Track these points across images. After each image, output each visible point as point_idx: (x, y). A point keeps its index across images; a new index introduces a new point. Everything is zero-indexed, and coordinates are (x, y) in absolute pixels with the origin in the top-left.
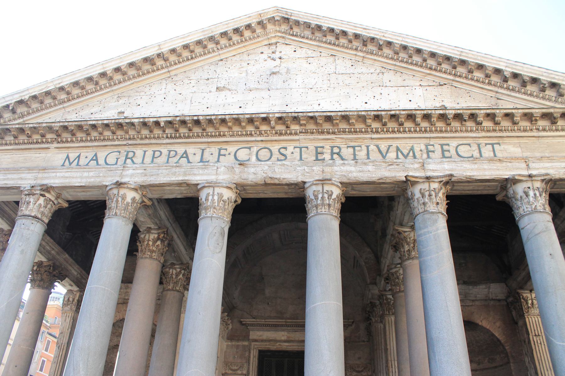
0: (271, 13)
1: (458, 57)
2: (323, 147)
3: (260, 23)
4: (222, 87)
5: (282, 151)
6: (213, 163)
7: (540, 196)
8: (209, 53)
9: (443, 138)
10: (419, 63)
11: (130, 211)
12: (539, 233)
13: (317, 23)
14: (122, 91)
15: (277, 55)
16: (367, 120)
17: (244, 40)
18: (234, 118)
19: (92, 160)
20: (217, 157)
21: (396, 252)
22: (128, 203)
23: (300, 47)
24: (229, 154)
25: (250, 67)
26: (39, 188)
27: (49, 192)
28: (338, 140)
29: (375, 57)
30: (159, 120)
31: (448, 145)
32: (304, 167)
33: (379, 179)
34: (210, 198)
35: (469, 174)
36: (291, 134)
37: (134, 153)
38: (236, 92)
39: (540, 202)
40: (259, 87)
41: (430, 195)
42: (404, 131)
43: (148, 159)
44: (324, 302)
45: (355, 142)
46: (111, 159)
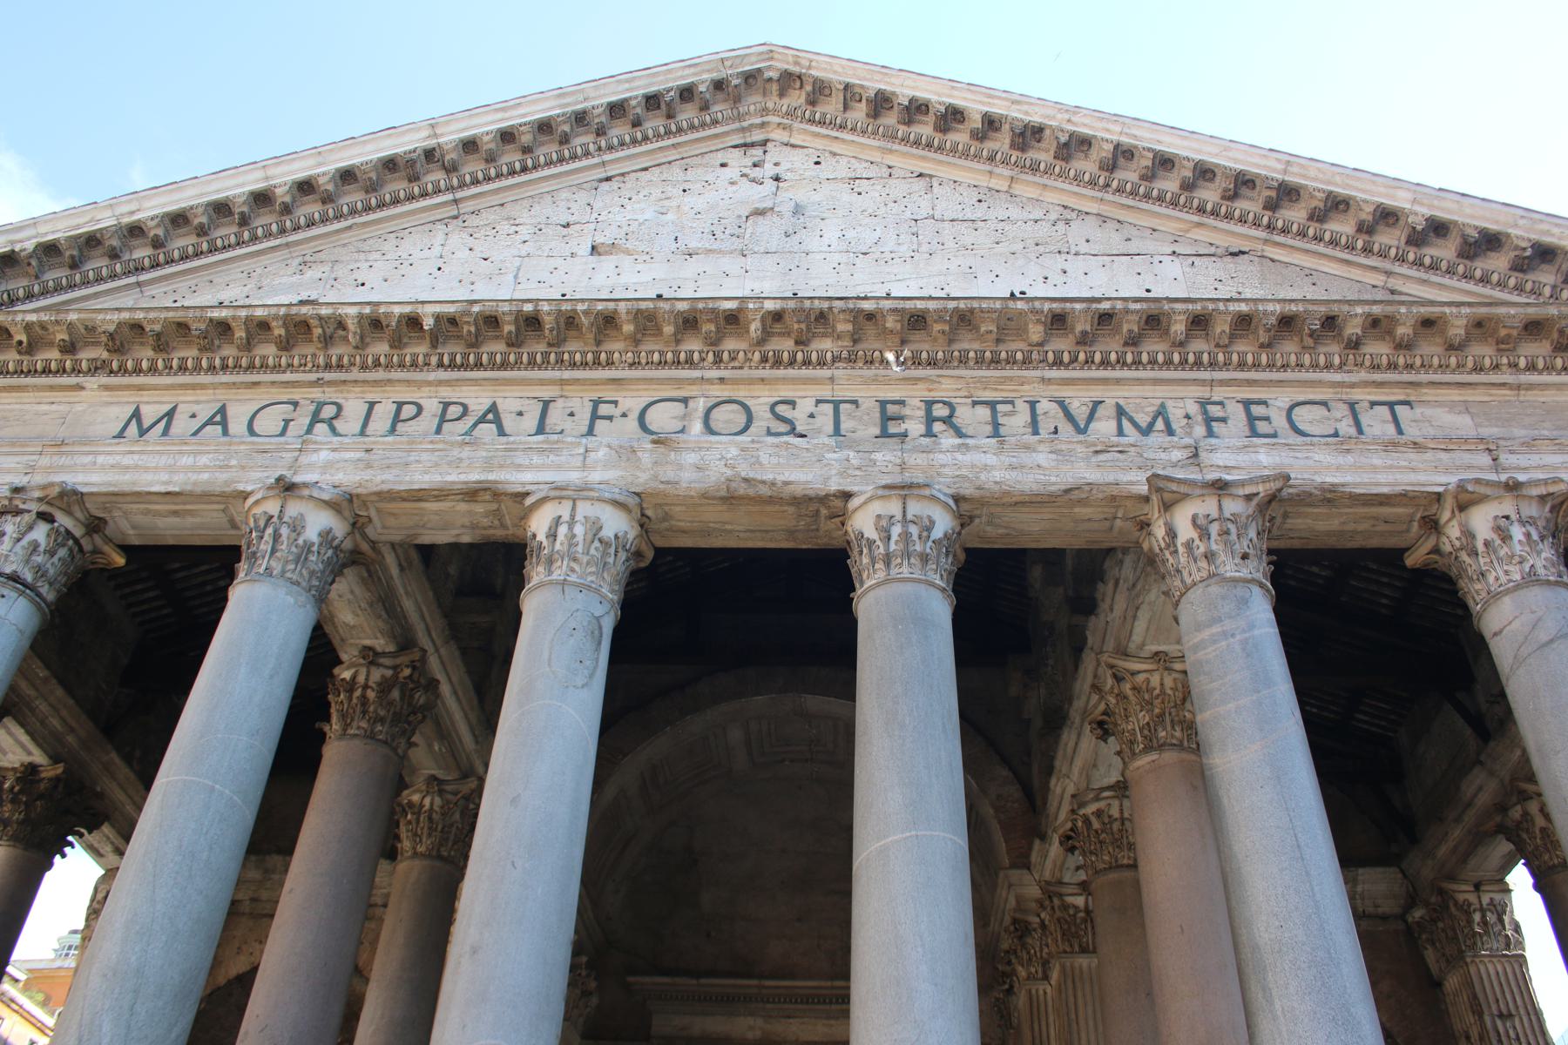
0: (754, 59)
1: (1280, 177)
2: (901, 403)
3: (719, 85)
4: (608, 245)
5: (781, 409)
7: (1542, 541)
8: (574, 157)
9: (1251, 383)
10: (1169, 195)
11: (313, 567)
12: (1551, 641)
13: (883, 87)
14: (316, 246)
16: (1030, 326)
17: (674, 128)
18: (639, 311)
19: (210, 422)
20: (587, 423)
21: (1105, 741)
22: (308, 547)
23: (831, 152)
24: (624, 415)
25: (689, 200)
26: (37, 494)
27: (69, 513)
29: (1044, 180)
30: (420, 310)
31: (1264, 403)
32: (846, 452)
33: (1067, 491)
34: (563, 530)
35: (1329, 479)
36: (807, 363)
37: (340, 408)
38: (647, 258)
39: (1544, 555)
40: (714, 247)
42: (1137, 363)
44: (913, 833)
45: (996, 389)
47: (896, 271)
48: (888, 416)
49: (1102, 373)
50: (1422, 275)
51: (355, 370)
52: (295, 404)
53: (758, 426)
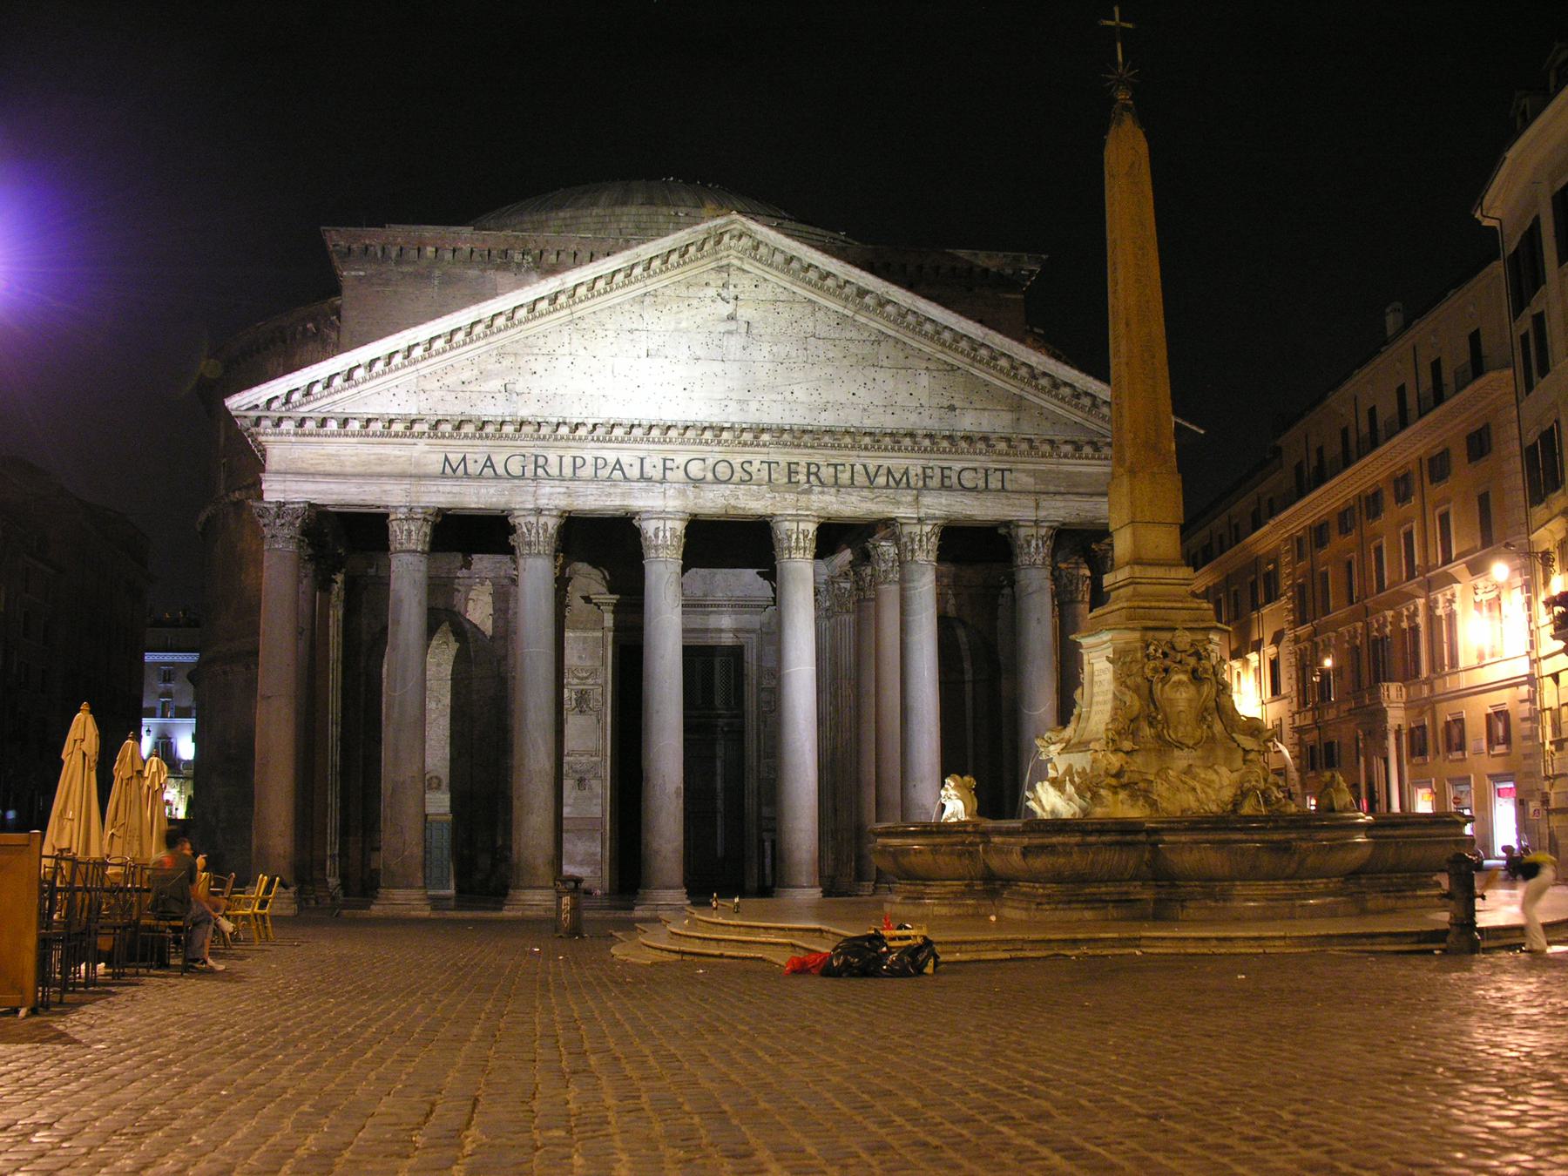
2: (797, 464)
6: (662, 483)
15: (732, 291)
19: (485, 466)
26: (420, 510)
28: (817, 456)
29: (871, 315)
31: (950, 468)
34: (661, 534)
36: (758, 445)
37: (546, 461)
38: (674, 361)
41: (920, 541)
42: (900, 449)
43: (568, 471)
46: (515, 469)
47: (796, 376)
48: (791, 471)
49: (883, 454)
50: (1035, 392)
51: (551, 440)
52: (524, 456)
53: (735, 474)
